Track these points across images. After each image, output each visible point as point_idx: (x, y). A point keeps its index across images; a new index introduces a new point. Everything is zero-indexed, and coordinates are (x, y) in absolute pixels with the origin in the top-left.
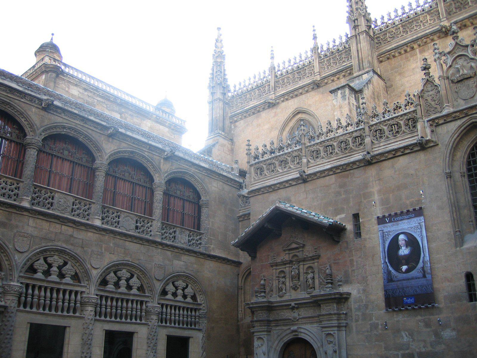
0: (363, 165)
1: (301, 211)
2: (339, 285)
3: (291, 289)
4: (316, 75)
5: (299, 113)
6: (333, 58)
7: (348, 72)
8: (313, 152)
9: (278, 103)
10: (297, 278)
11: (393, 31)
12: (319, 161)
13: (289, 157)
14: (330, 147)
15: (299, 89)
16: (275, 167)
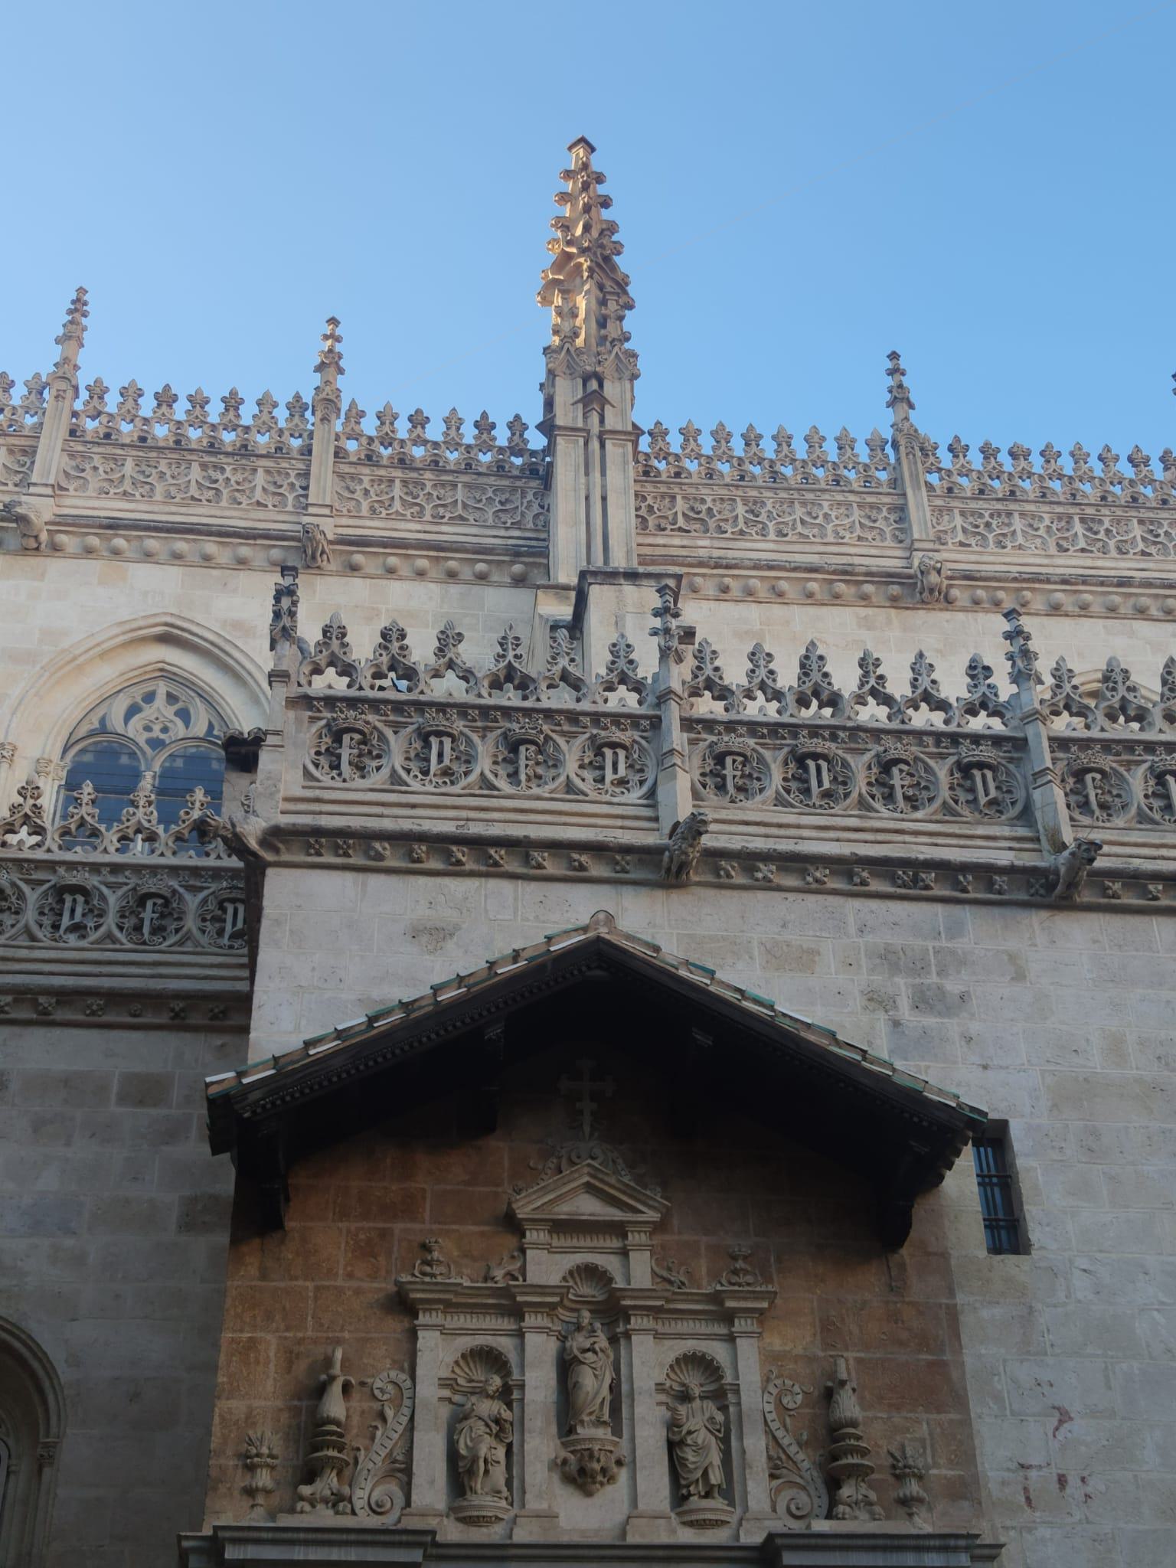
0: (1023, 896)
1: (773, 1010)
2: (905, 1502)
3: (556, 1477)
4: (311, 510)
5: (165, 639)
6: (405, 482)
7: (481, 567)
8: (720, 759)
9: (56, 548)
10: (606, 1417)
11: (703, 501)
12: (756, 808)
13: (563, 733)
14: (824, 765)
15: (210, 534)
16: (469, 760)
